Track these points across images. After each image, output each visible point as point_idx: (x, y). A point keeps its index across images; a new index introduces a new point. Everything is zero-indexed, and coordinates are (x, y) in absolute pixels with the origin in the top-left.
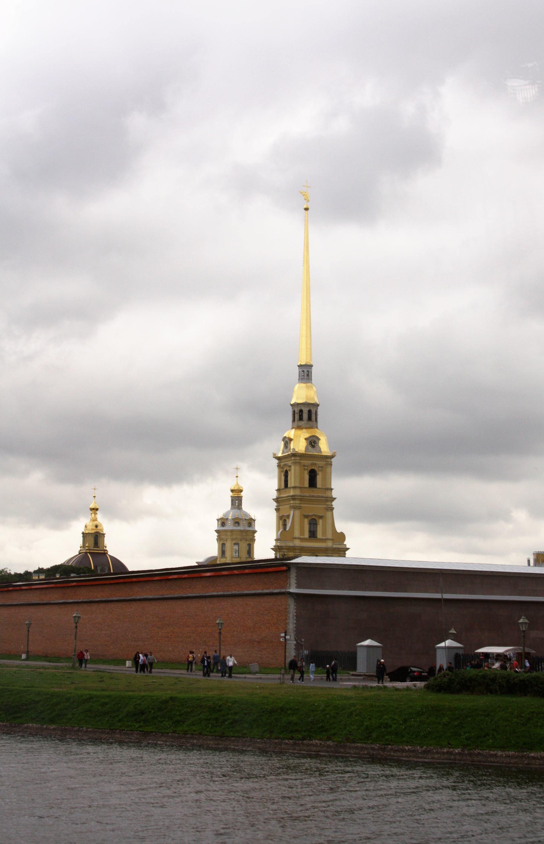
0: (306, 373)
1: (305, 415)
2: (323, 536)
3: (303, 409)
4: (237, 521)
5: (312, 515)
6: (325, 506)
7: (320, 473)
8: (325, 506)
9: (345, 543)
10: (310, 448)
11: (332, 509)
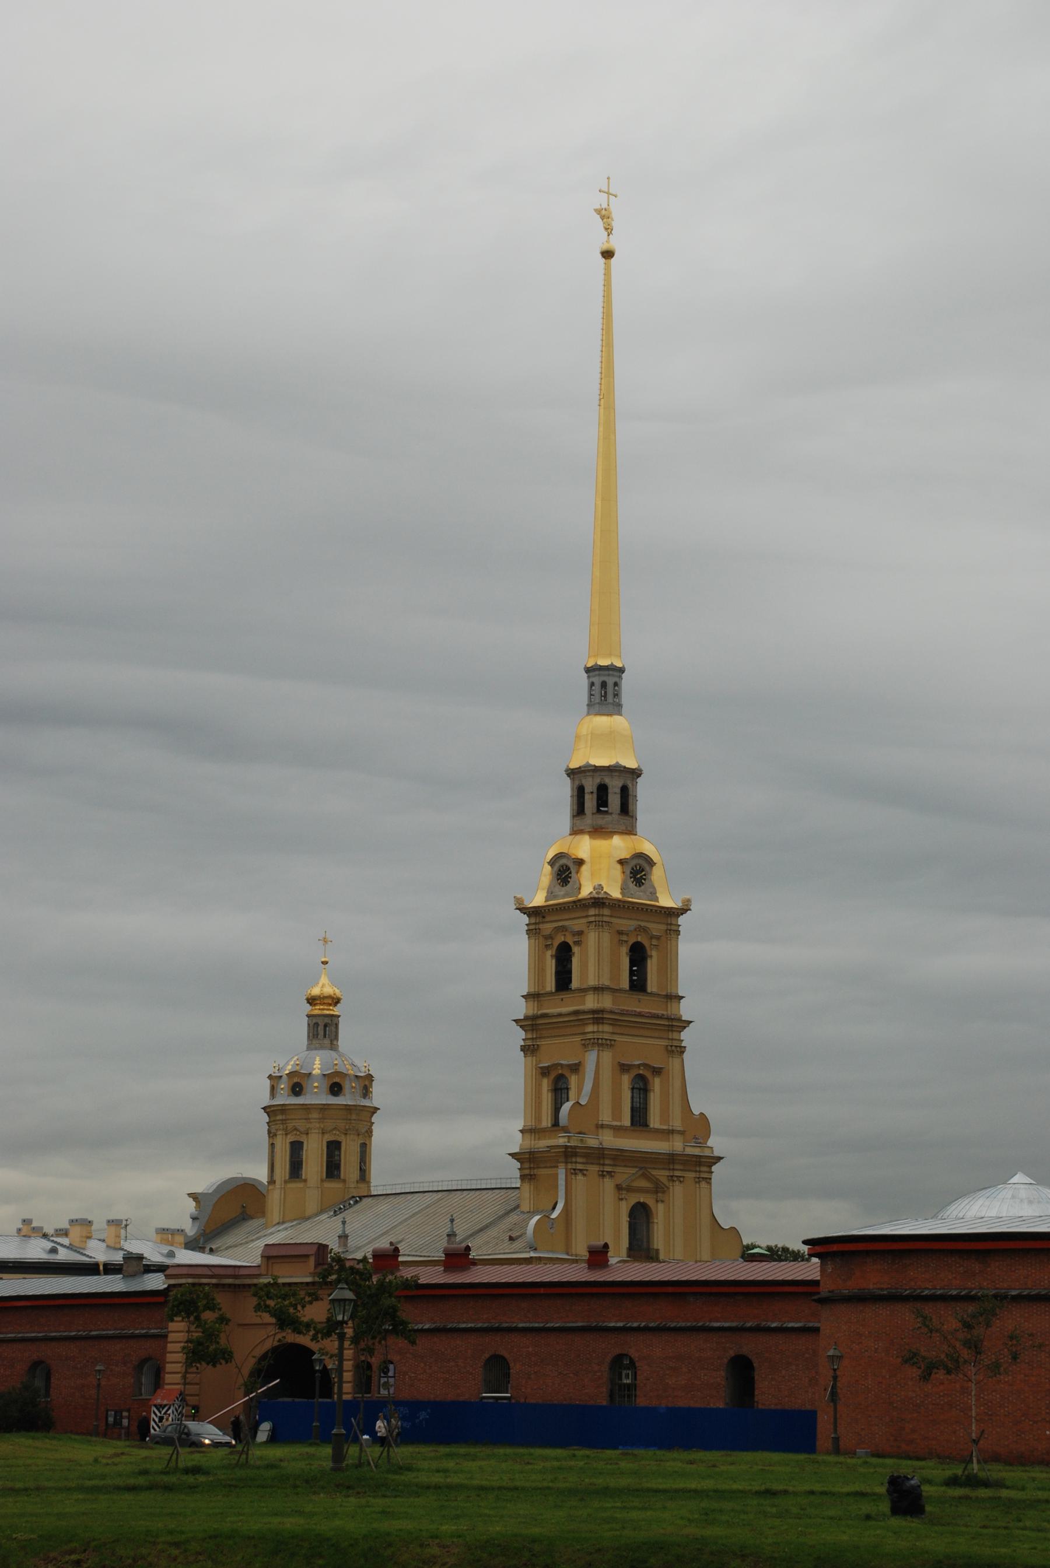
0: (605, 688)
1: (604, 798)
2: (613, 1119)
3: (607, 781)
4: (337, 1080)
5: (639, 1066)
6: (665, 1043)
7: (654, 953)
8: (665, 1043)
9: (710, 1143)
10: (632, 886)
11: (681, 1050)
